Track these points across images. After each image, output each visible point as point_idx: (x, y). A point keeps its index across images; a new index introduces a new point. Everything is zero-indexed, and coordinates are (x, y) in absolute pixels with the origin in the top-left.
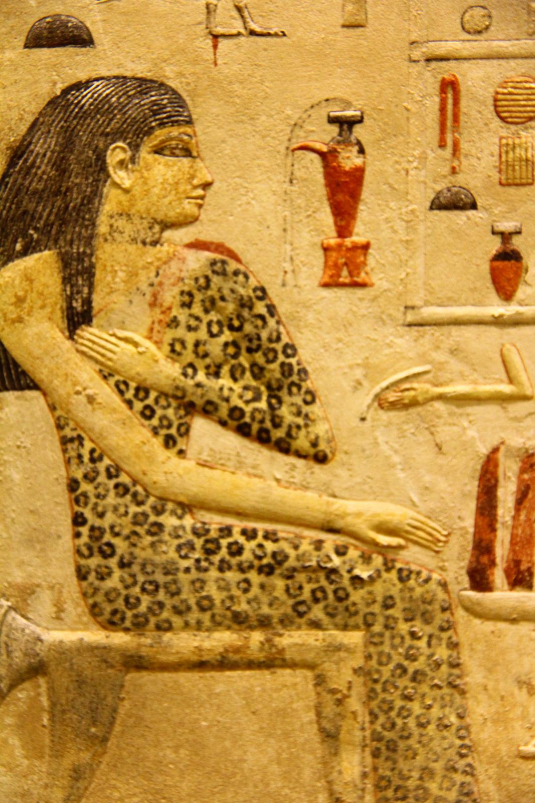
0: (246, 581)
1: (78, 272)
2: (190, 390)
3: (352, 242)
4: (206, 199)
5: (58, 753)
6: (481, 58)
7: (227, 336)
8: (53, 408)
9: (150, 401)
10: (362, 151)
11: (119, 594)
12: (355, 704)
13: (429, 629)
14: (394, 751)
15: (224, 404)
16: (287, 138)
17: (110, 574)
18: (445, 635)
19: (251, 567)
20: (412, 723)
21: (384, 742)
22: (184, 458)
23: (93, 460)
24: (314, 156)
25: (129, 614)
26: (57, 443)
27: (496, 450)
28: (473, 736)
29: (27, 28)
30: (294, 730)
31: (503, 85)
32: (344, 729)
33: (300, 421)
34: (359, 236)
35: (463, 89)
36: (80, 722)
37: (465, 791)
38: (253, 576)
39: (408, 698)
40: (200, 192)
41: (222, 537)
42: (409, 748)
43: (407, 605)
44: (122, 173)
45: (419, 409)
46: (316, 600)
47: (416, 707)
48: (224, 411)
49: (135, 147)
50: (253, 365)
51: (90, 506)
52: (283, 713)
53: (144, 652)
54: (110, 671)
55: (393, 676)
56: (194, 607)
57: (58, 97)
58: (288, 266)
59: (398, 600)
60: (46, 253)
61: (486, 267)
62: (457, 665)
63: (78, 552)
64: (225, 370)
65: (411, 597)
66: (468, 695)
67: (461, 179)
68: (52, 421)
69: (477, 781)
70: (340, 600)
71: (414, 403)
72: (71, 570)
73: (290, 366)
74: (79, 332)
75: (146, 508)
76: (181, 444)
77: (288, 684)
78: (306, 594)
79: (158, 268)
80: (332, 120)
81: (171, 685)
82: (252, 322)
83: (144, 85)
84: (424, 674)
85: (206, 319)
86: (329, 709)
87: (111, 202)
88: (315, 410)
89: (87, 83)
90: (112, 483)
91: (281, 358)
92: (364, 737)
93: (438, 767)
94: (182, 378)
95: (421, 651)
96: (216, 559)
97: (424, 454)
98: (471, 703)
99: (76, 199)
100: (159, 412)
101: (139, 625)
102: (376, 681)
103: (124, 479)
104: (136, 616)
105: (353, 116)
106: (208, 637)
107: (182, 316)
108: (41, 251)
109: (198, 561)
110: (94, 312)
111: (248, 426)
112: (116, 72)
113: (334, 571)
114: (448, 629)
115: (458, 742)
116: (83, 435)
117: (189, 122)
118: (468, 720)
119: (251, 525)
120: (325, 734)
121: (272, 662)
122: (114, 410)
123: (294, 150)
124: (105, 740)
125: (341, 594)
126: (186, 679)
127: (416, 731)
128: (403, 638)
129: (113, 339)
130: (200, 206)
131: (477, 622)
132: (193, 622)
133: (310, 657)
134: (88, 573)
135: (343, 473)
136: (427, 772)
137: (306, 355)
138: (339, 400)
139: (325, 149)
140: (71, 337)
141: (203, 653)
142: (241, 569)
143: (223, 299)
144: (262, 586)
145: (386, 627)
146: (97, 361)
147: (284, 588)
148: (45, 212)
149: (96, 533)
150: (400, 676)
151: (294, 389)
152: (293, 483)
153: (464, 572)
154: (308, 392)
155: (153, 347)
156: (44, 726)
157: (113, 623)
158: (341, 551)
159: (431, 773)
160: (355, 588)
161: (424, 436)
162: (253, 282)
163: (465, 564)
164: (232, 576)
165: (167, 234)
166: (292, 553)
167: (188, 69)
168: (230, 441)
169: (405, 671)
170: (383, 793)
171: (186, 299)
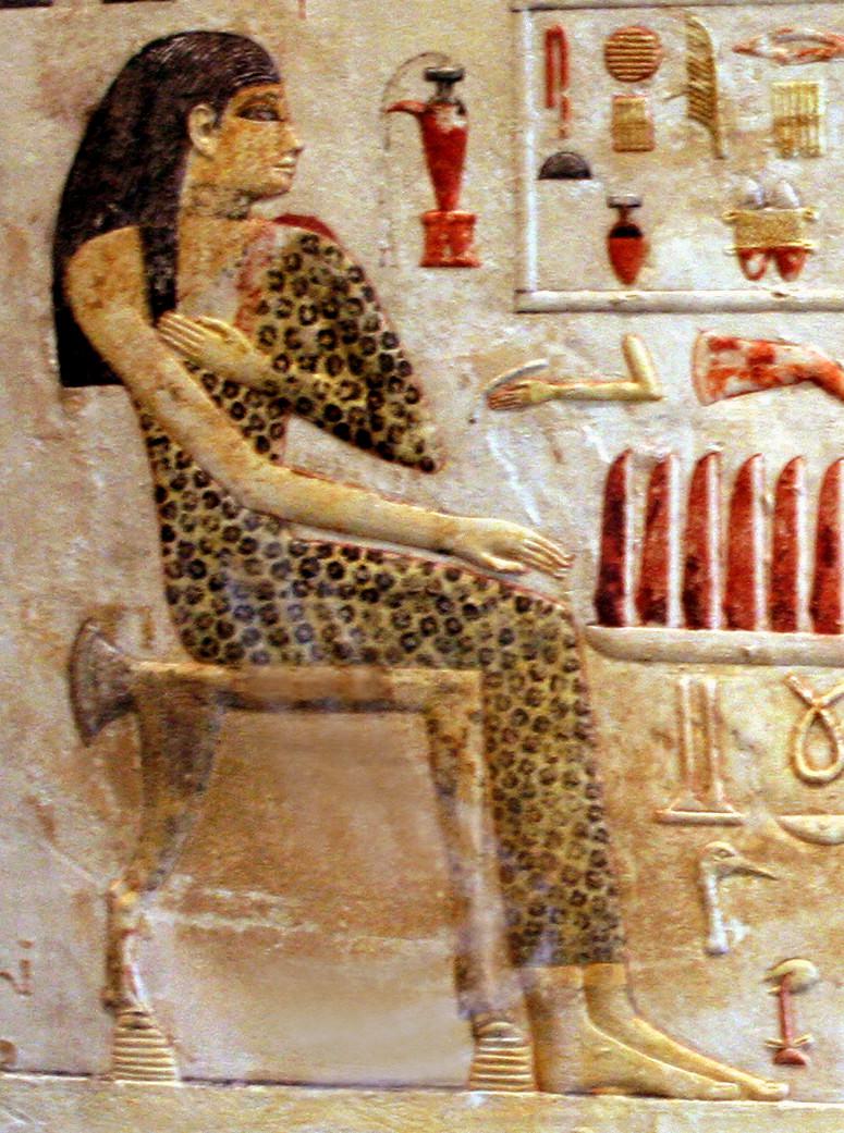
0: (348, 608)
1: (160, 248)
2: (283, 385)
3: (456, 216)
4: (298, 168)
5: (150, 804)
6: (592, 8)
7: (320, 325)
8: (137, 404)
9: (239, 398)
10: (462, 112)
11: (211, 621)
12: (474, 755)
13: (552, 670)
15: (319, 402)
16: (380, 97)
18: (571, 677)
19: (353, 592)
20: (535, 779)
22: (275, 464)
24: (409, 118)
25: (223, 644)
26: (142, 448)
27: (621, 460)
31: (614, 37)
32: (460, 784)
33: (401, 421)
34: (463, 208)
35: (570, 40)
38: (359, 605)
39: (529, 749)
40: (288, 159)
41: (320, 557)
42: (533, 809)
44: (205, 140)
45: (533, 411)
46: (426, 633)
47: (539, 761)
48: (319, 412)
49: (219, 109)
50: (352, 357)
51: (178, 519)
53: (241, 688)
54: (204, 709)
55: (513, 724)
57: (138, 56)
59: (516, 634)
60: (127, 230)
62: (586, 713)
63: (167, 572)
64: (321, 364)
67: (571, 144)
68: (136, 421)
70: (452, 632)
71: (525, 405)
73: (390, 357)
74: (163, 319)
76: (275, 447)
78: (415, 625)
79: (245, 245)
80: (431, 77)
82: (348, 308)
83: (226, 40)
84: (547, 722)
87: (192, 172)
90: (201, 492)
91: (381, 350)
93: (566, 830)
94: (272, 371)
96: (314, 581)
97: (541, 464)
98: (602, 758)
99: (155, 168)
100: (251, 411)
101: (233, 657)
102: (494, 729)
103: (213, 487)
104: (230, 646)
105: (450, 73)
107: (272, 300)
108: (119, 227)
110: (179, 295)
113: (442, 599)
115: (588, 802)
116: (170, 437)
117: (276, 80)
118: (599, 778)
121: (383, 703)
122: (202, 409)
123: (390, 111)
128: (522, 679)
129: (198, 327)
130: (290, 175)
131: (606, 662)
132: (292, 654)
133: (421, 698)
135: (451, 483)
136: (554, 837)
139: (421, 110)
140: (155, 324)
142: (344, 593)
143: (315, 280)
144: (366, 615)
145: (506, 666)
146: (183, 353)
148: (124, 181)
151: (396, 386)
152: (398, 496)
154: (411, 389)
155: (238, 334)
157: (205, 654)
161: (542, 443)
163: (590, 592)
165: (257, 207)
166: (399, 577)
167: (274, 22)
171: (276, 280)
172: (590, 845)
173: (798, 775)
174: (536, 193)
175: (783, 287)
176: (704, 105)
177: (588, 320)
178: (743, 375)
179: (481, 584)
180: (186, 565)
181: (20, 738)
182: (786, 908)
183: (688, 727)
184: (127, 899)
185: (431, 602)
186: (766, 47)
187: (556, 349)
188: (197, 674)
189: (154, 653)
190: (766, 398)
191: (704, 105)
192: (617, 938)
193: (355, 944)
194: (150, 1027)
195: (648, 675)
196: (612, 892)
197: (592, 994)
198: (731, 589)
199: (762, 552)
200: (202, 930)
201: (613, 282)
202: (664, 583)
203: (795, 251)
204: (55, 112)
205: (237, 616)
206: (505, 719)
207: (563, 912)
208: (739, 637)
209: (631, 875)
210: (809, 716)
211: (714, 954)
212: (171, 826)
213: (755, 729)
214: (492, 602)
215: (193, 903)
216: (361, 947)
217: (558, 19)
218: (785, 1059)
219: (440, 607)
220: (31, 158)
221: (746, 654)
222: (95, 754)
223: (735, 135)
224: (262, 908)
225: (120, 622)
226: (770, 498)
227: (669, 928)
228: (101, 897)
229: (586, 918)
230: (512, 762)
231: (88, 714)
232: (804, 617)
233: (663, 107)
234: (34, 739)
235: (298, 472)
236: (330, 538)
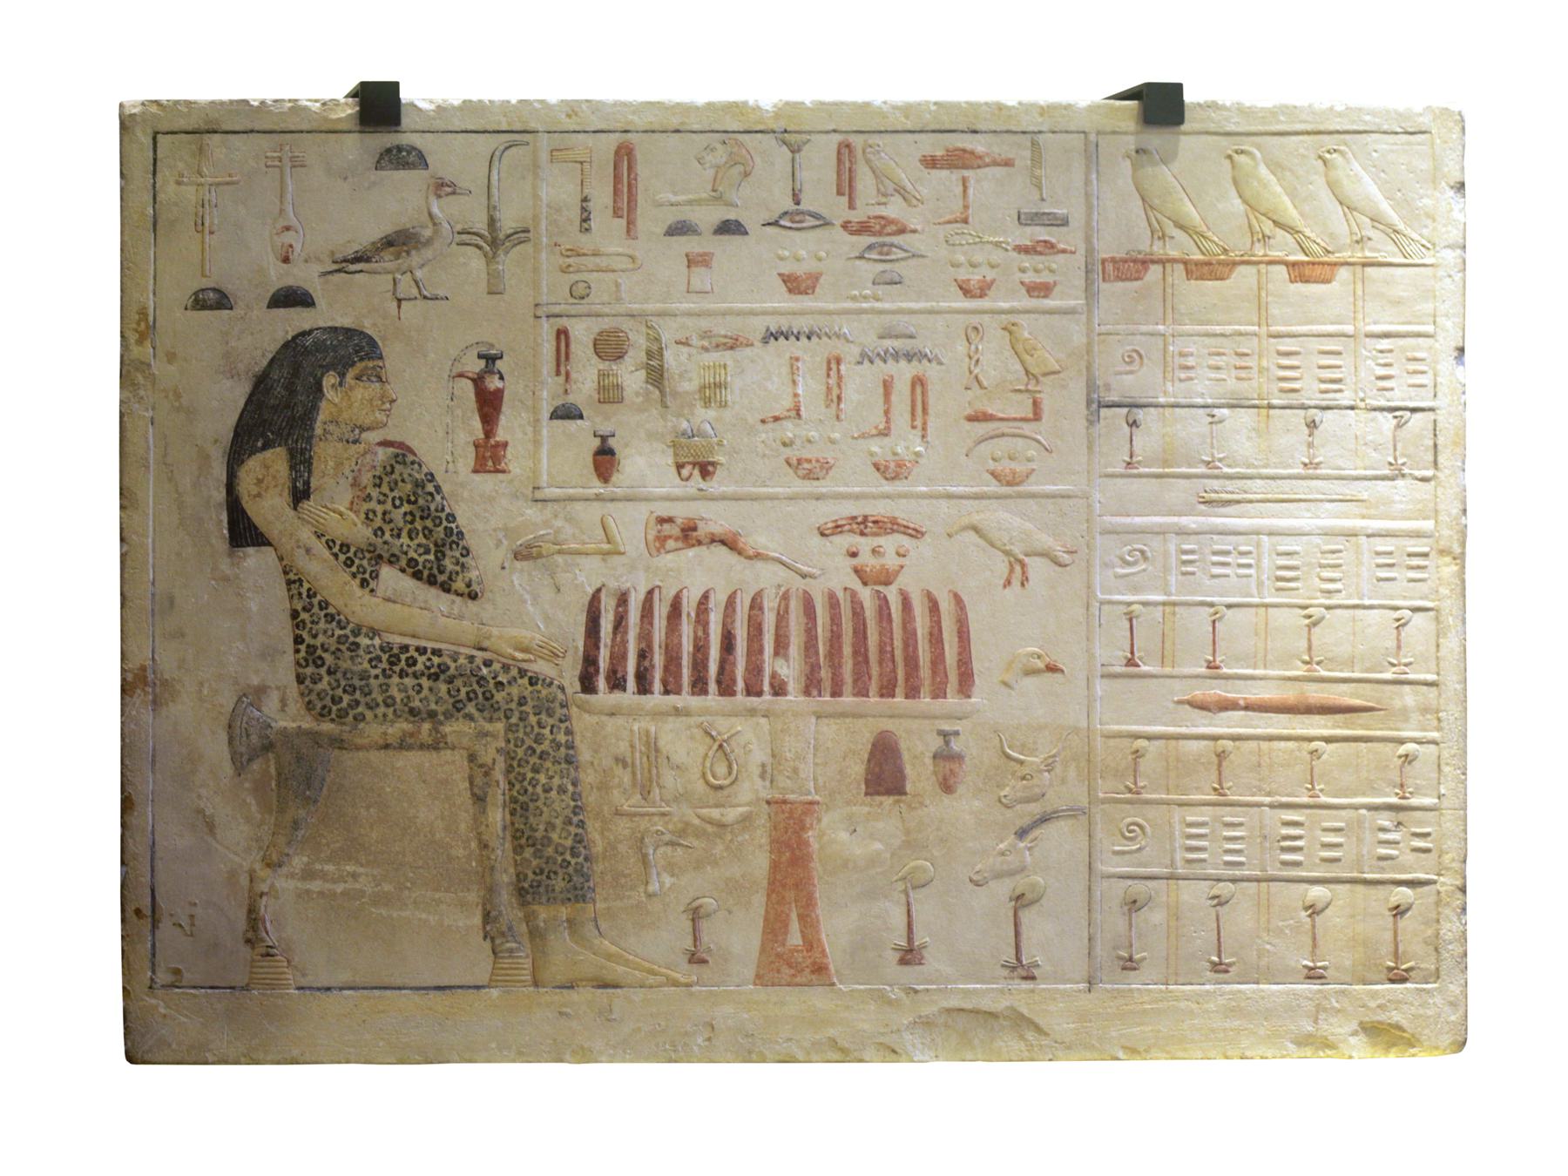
0: (420, 685)
1: (301, 461)
7: (406, 508)
8: (281, 559)
9: (351, 554)
10: (502, 378)
12: (498, 774)
13: (551, 721)
20: (539, 789)
23: (309, 596)
27: (599, 590)
29: (269, 295)
33: (458, 568)
35: (571, 334)
38: (425, 682)
39: (536, 770)
46: (470, 700)
47: (542, 778)
48: (403, 563)
49: (342, 375)
50: (425, 528)
53: (345, 736)
58: (449, 458)
61: (590, 459)
63: (298, 663)
64: (404, 534)
67: (571, 399)
70: (487, 699)
71: (540, 556)
72: (293, 677)
75: (347, 631)
76: (373, 584)
80: (480, 356)
83: (348, 332)
85: (391, 495)
88: (468, 561)
89: (310, 332)
91: (445, 523)
93: (558, 822)
96: (397, 669)
97: (547, 594)
98: (582, 776)
100: (357, 561)
103: (331, 610)
107: (375, 493)
109: (384, 670)
111: (420, 572)
112: (330, 324)
113: (483, 678)
117: (381, 358)
119: (423, 643)
121: (436, 746)
124: (316, 801)
126: (376, 757)
127: (542, 796)
131: (586, 716)
133: (465, 741)
136: (550, 826)
137: (462, 521)
138: (487, 556)
140: (295, 509)
142: (415, 676)
144: (431, 689)
149: (311, 649)
155: (352, 515)
157: (323, 714)
158: (488, 663)
159: (554, 827)
162: (425, 470)
163: (577, 673)
164: (409, 681)
165: (364, 435)
166: (453, 665)
168: (407, 583)
172: (573, 830)
173: (707, 783)
174: (549, 428)
175: (702, 485)
176: (656, 375)
177: (578, 506)
178: (677, 539)
179: (506, 668)
180: (309, 656)
182: (698, 866)
183: (638, 755)
184: (262, 873)
185: (474, 679)
186: (695, 341)
187: (559, 523)
189: (286, 714)
190: (691, 553)
191: (656, 375)
195: (611, 724)
196: (586, 859)
197: (571, 922)
198: (666, 669)
199: (687, 647)
201: (596, 482)
202: (625, 667)
203: (713, 464)
204: (233, 374)
205: (345, 691)
206: (520, 752)
208: (672, 699)
209: (598, 848)
210: (715, 747)
211: (649, 896)
212: (296, 825)
213: (679, 756)
215: (308, 874)
217: (564, 322)
218: (696, 959)
219: (473, 686)
220: (215, 404)
221: (676, 709)
223: (675, 394)
224: (354, 876)
226: (693, 614)
227: (623, 881)
232: (712, 687)
233: (631, 377)
235: (388, 600)
236: (407, 641)
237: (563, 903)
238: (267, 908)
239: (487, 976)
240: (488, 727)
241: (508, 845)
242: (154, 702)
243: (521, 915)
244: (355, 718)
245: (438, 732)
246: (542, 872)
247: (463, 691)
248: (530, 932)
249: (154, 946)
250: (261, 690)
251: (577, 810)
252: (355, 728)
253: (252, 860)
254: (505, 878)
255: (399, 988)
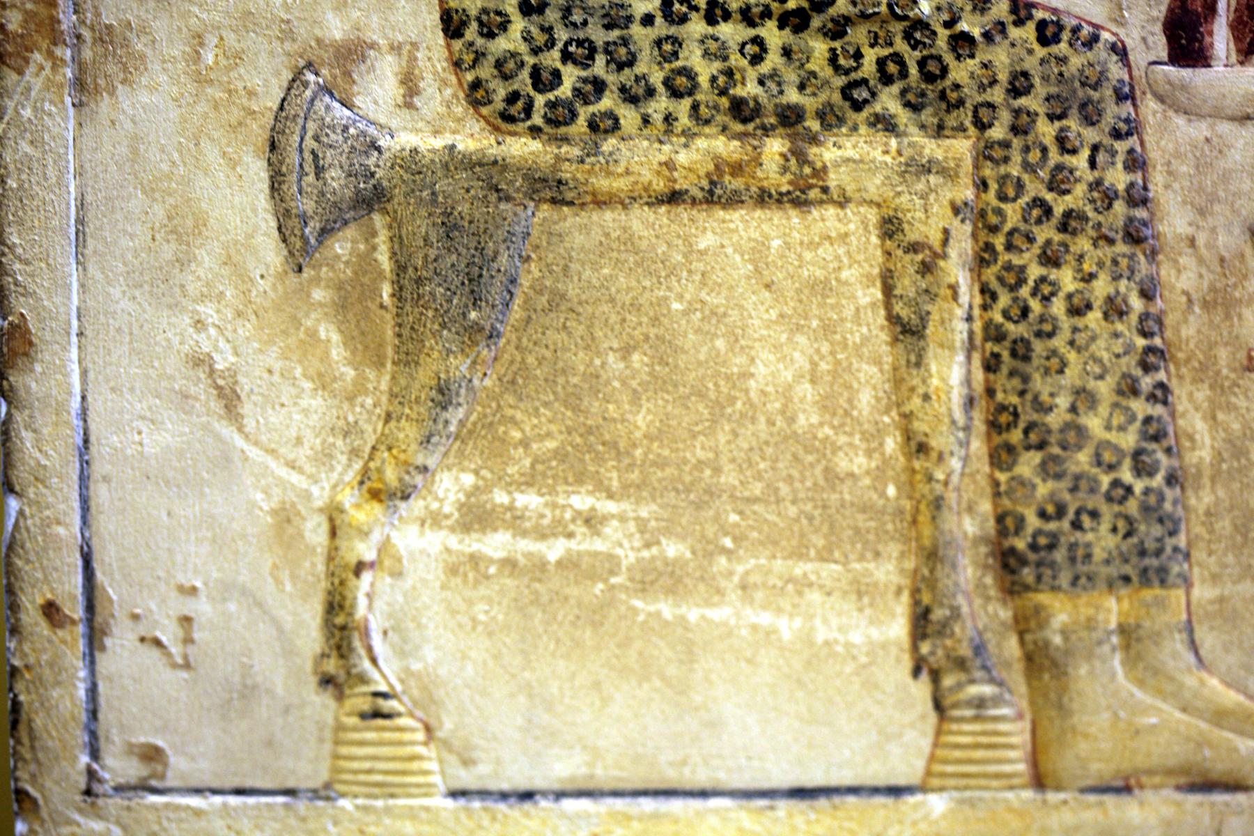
0: (758, 41)
5: (408, 359)
11: (522, 64)
12: (956, 270)
13: (1092, 135)
14: (1026, 358)
17: (504, 26)
18: (1121, 147)
20: (1058, 307)
21: (1007, 344)
25: (540, 100)
28: (1168, 334)
30: (842, 320)
32: (935, 316)
36: (450, 301)
37: (1151, 431)
38: (773, 35)
39: (1050, 259)
42: (1054, 353)
43: (1054, 90)
46: (887, 80)
47: (1067, 279)
52: (821, 288)
56: (661, 89)
59: (1037, 81)
62: (1144, 202)
65: (1061, 74)
66: (1160, 257)
69: (1173, 414)
77: (833, 234)
78: (868, 66)
81: (614, 235)
84: (1083, 218)
86: (907, 282)
92: (971, 334)
95: (1078, 174)
98: (1166, 272)
102: (994, 229)
104: (552, 105)
106: (686, 146)
114: (1129, 134)
115: (1141, 342)
120: (899, 329)
124: (493, 335)
125: (933, 67)
126: (644, 223)
127: (1065, 323)
128: (1044, 150)
131: (1180, 121)
133: (874, 185)
134: (464, 24)
141: (676, 174)
144: (787, 52)
145: (1015, 130)
147: (827, 55)
150: (1039, 221)
153: (1158, 28)
156: (382, 306)
157: (511, 116)
160: (958, 58)
164: (731, 32)
169: (1048, 211)
170: (1005, 436)
172: (1140, 407)
181: (183, 262)
185: (897, 28)
188: (494, 151)
189: (415, 116)
192: (1176, 549)
193: (747, 573)
194: (399, 715)
196: (1171, 480)
200: (491, 561)
205: (566, 57)
206: (1013, 214)
207: (1094, 515)
212: (444, 395)
214: (1001, 26)
215: (476, 517)
216: (753, 579)
222: (316, 281)
224: (591, 521)
225: (363, 67)
228: (321, 510)
229: (1129, 520)
230: (1021, 281)
231: (304, 219)
234: (207, 260)
237: (1111, 586)
238: (372, 602)
239: (920, 765)
240: (932, 148)
241: (978, 446)
242: (80, 84)
243: (1005, 614)
244: (593, 126)
245: (802, 159)
246: (1061, 511)
247: (870, 56)
248: (1029, 658)
249: (93, 691)
250: (352, 54)
251: (1150, 359)
252: (595, 150)
253: (337, 483)
254: (970, 527)
255: (703, 794)
